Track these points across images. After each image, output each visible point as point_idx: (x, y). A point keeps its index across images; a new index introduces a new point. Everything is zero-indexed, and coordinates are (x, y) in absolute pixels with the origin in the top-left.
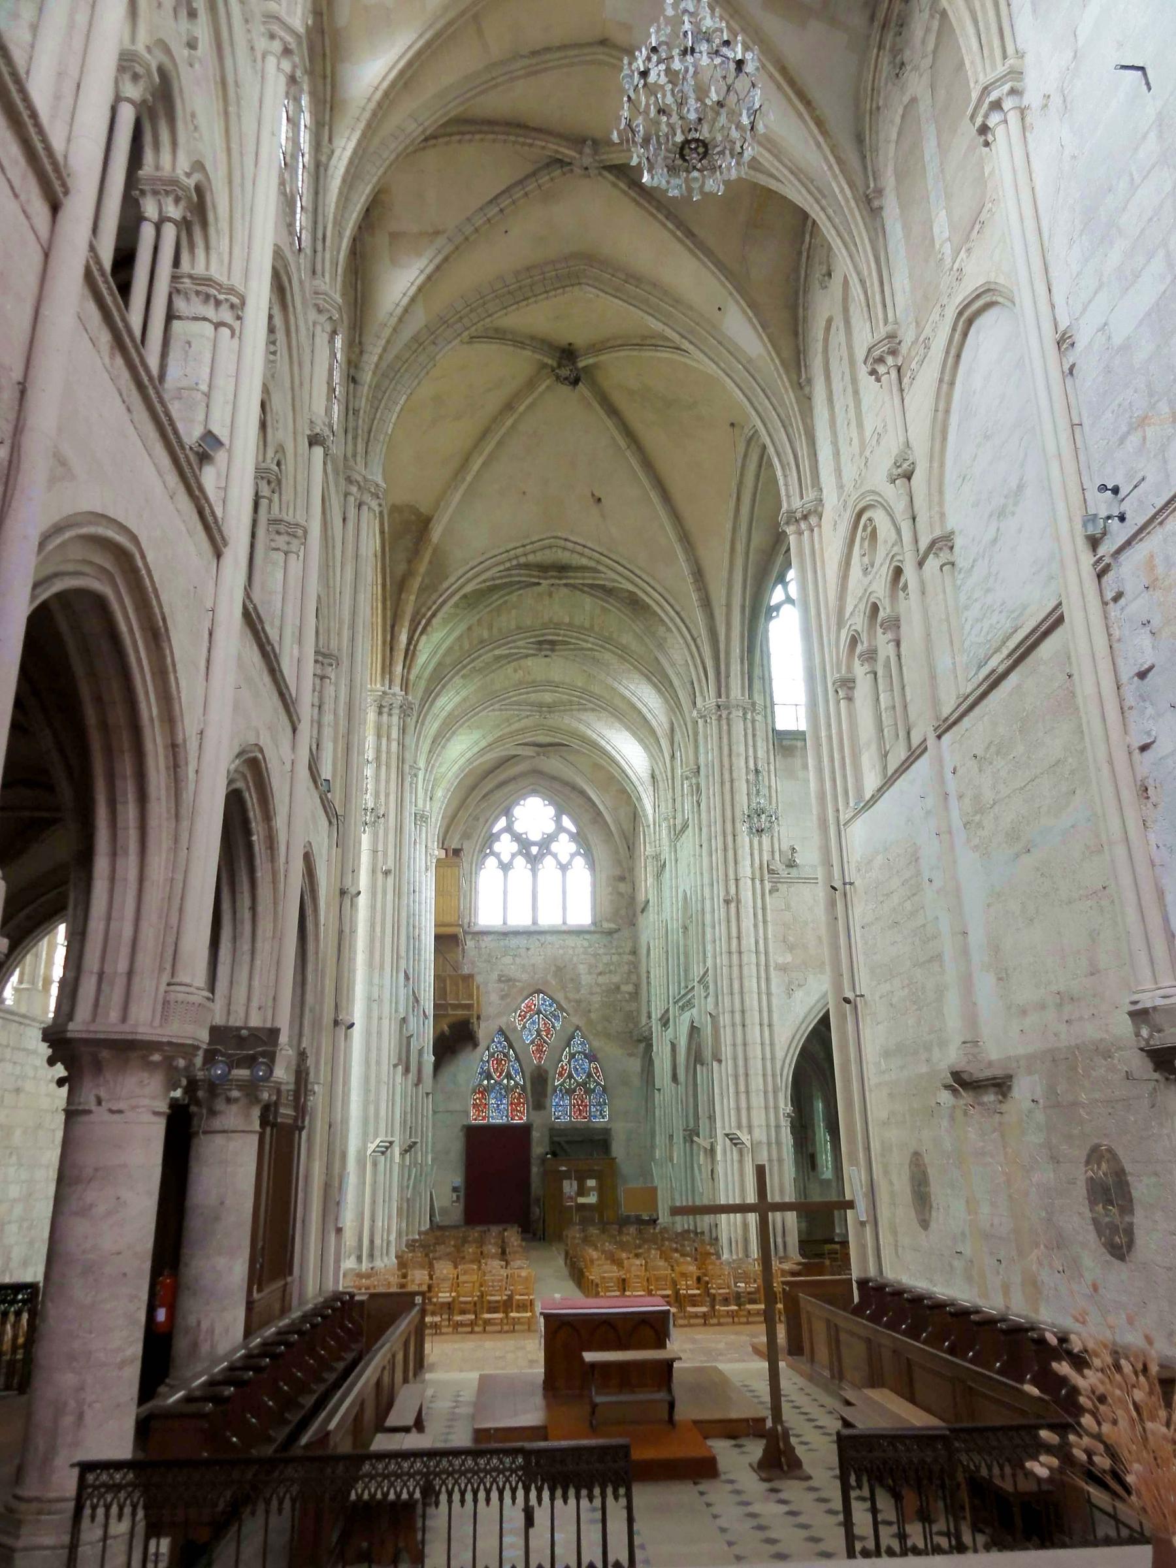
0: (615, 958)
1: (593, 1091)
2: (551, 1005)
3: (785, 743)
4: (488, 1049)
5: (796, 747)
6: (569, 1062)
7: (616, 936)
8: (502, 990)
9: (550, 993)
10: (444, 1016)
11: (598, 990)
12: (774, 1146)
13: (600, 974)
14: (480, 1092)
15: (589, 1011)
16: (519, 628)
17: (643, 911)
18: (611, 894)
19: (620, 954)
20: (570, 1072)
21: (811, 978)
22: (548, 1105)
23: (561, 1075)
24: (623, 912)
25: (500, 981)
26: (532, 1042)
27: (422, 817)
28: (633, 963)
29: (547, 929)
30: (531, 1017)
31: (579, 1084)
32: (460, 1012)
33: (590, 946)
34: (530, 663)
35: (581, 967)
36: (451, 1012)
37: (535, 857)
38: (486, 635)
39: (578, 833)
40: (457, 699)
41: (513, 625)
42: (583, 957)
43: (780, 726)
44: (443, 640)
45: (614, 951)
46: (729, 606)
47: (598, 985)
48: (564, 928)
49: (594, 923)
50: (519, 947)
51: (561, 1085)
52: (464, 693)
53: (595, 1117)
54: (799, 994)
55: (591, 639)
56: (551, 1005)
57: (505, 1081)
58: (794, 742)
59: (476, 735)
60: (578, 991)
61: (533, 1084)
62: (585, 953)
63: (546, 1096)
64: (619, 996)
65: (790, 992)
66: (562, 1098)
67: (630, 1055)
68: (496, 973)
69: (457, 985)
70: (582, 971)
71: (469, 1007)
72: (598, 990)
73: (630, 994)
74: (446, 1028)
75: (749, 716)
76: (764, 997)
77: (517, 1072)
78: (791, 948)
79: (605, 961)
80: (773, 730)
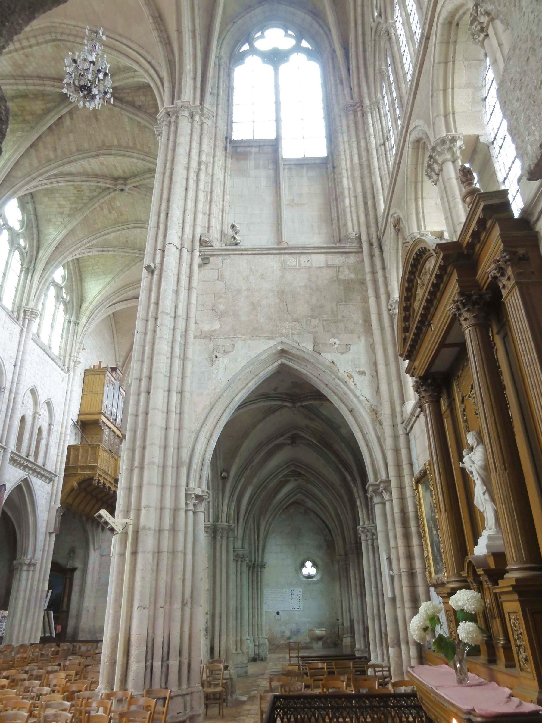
3: (239, 150)
5: (251, 153)
10: (76, 475)
12: (166, 534)
16: (78, 150)
21: (239, 344)
27: (32, 314)
32: (87, 472)
34: (118, 204)
36: (79, 472)
38: (52, 155)
40: (65, 232)
41: (74, 148)
43: (236, 136)
44: (11, 156)
46: (179, 31)
52: (70, 227)
54: (223, 361)
55: (135, 155)
58: (248, 149)
59: (108, 279)
65: (213, 359)
69: (87, 452)
71: (94, 468)
74: (75, 484)
75: (197, 118)
76: (177, 363)
78: (220, 316)
80: (228, 139)
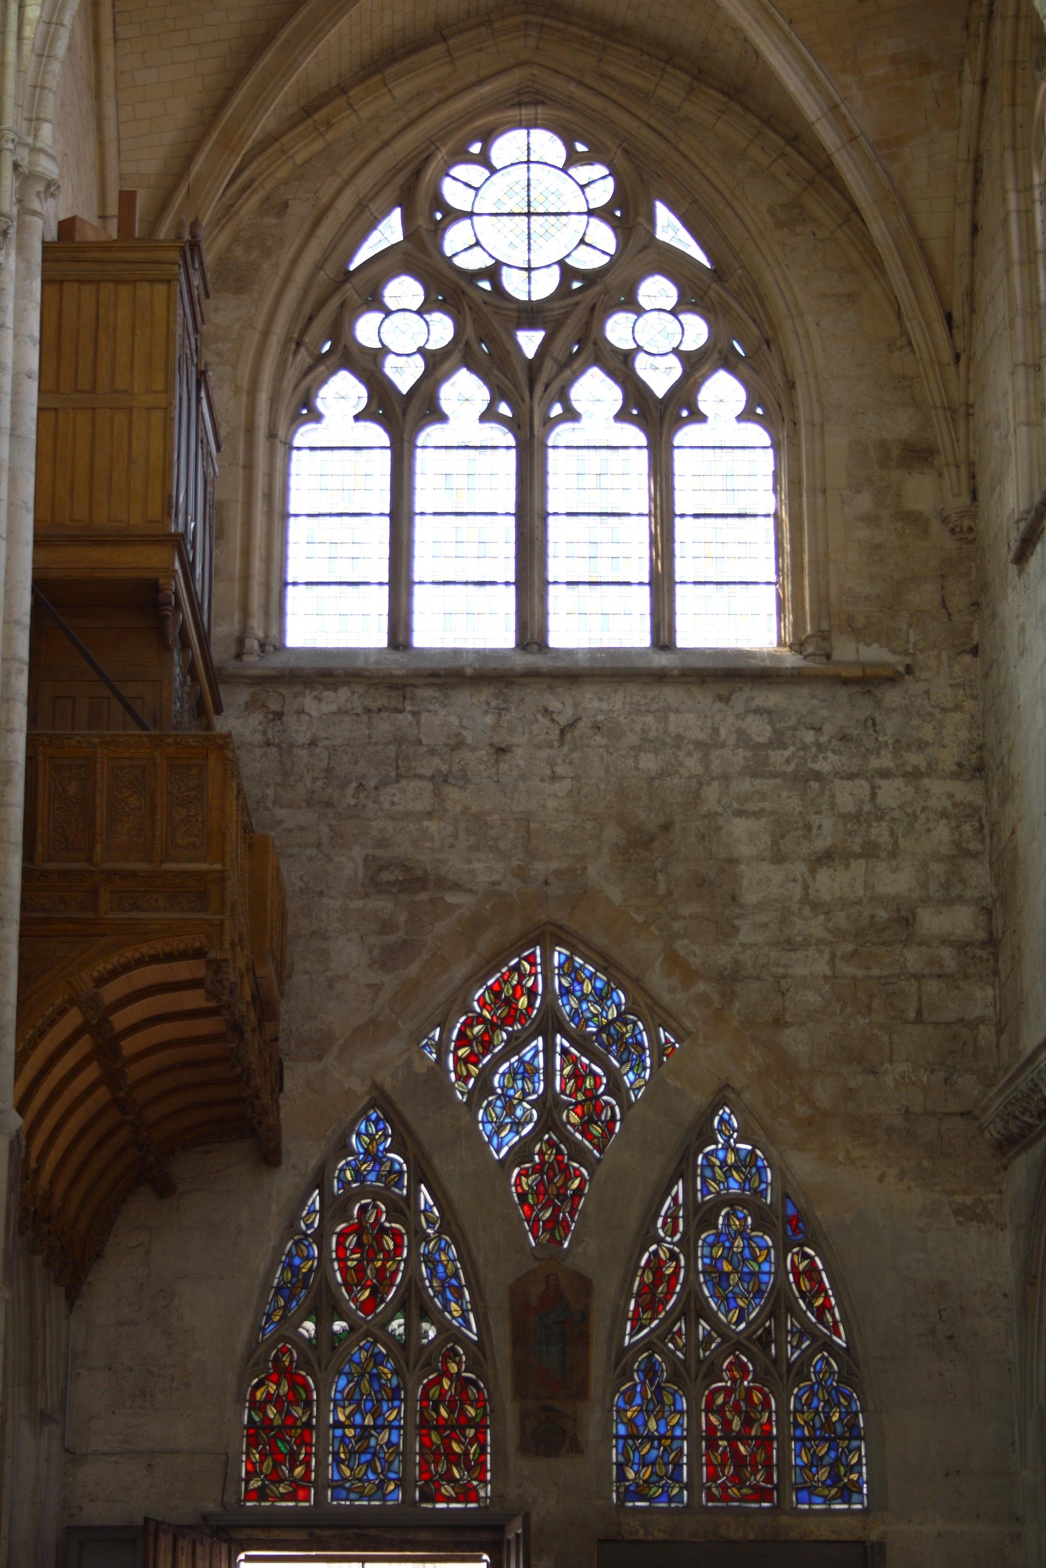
0: (891, 792)
1: (799, 1371)
2: (601, 997)
4: (320, 1181)
6: (688, 1244)
7: (892, 697)
8: (386, 926)
9: (600, 940)
11: (816, 927)
13: (825, 858)
14: (280, 1372)
15: (779, 1022)
17: (1021, 557)
18: (871, 520)
19: (914, 775)
20: (692, 1292)
22: (591, 1433)
23: (650, 1301)
24: (924, 596)
25: (374, 885)
26: (521, 1153)
28: (974, 811)
29: (583, 662)
30: (515, 1045)
31: (732, 1344)
33: (778, 741)
35: (740, 827)
37: (533, 367)
39: (719, 273)
42: (746, 785)
45: (886, 761)
47: (817, 907)
48: (662, 660)
49: (798, 646)
50: (458, 744)
51: (647, 1345)
53: (810, 1490)
56: (601, 997)
57: (397, 1326)
60: (727, 932)
61: (519, 1340)
62: (757, 769)
63: (582, 1393)
64: (913, 958)
66: (656, 1406)
67: (966, 1214)
68: (358, 852)
70: (744, 850)
72: (816, 927)
73: (962, 946)
77: (448, 1287)
79: (846, 803)
